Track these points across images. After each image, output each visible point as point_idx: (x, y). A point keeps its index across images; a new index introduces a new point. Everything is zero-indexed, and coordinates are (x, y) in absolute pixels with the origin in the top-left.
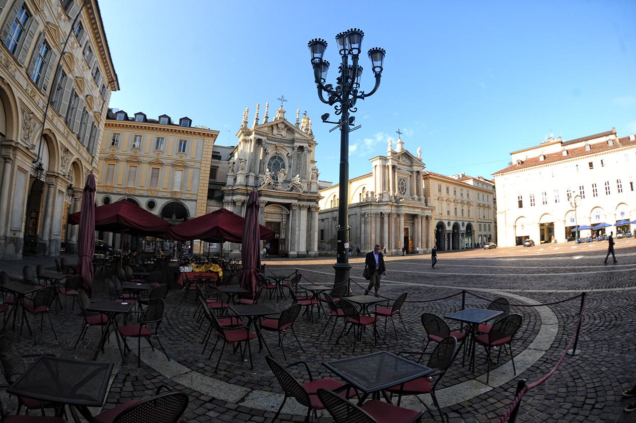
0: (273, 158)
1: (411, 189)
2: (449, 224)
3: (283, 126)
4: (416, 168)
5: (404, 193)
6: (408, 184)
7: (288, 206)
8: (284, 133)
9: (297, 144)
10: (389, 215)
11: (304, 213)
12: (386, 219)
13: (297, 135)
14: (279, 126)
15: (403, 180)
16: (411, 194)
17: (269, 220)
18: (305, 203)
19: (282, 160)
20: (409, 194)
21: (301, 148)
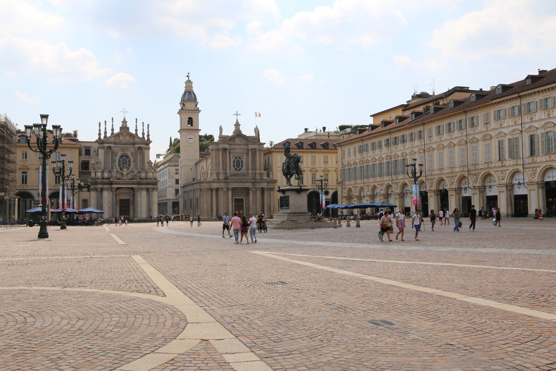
0: (122, 156)
3: (126, 134)
4: (251, 147)
6: (244, 161)
7: (132, 189)
8: (128, 138)
9: (137, 146)
10: (217, 190)
11: (144, 193)
13: (137, 140)
14: (123, 134)
15: (240, 158)
16: (248, 169)
18: (144, 186)
19: (127, 157)
20: (245, 169)
21: (140, 148)
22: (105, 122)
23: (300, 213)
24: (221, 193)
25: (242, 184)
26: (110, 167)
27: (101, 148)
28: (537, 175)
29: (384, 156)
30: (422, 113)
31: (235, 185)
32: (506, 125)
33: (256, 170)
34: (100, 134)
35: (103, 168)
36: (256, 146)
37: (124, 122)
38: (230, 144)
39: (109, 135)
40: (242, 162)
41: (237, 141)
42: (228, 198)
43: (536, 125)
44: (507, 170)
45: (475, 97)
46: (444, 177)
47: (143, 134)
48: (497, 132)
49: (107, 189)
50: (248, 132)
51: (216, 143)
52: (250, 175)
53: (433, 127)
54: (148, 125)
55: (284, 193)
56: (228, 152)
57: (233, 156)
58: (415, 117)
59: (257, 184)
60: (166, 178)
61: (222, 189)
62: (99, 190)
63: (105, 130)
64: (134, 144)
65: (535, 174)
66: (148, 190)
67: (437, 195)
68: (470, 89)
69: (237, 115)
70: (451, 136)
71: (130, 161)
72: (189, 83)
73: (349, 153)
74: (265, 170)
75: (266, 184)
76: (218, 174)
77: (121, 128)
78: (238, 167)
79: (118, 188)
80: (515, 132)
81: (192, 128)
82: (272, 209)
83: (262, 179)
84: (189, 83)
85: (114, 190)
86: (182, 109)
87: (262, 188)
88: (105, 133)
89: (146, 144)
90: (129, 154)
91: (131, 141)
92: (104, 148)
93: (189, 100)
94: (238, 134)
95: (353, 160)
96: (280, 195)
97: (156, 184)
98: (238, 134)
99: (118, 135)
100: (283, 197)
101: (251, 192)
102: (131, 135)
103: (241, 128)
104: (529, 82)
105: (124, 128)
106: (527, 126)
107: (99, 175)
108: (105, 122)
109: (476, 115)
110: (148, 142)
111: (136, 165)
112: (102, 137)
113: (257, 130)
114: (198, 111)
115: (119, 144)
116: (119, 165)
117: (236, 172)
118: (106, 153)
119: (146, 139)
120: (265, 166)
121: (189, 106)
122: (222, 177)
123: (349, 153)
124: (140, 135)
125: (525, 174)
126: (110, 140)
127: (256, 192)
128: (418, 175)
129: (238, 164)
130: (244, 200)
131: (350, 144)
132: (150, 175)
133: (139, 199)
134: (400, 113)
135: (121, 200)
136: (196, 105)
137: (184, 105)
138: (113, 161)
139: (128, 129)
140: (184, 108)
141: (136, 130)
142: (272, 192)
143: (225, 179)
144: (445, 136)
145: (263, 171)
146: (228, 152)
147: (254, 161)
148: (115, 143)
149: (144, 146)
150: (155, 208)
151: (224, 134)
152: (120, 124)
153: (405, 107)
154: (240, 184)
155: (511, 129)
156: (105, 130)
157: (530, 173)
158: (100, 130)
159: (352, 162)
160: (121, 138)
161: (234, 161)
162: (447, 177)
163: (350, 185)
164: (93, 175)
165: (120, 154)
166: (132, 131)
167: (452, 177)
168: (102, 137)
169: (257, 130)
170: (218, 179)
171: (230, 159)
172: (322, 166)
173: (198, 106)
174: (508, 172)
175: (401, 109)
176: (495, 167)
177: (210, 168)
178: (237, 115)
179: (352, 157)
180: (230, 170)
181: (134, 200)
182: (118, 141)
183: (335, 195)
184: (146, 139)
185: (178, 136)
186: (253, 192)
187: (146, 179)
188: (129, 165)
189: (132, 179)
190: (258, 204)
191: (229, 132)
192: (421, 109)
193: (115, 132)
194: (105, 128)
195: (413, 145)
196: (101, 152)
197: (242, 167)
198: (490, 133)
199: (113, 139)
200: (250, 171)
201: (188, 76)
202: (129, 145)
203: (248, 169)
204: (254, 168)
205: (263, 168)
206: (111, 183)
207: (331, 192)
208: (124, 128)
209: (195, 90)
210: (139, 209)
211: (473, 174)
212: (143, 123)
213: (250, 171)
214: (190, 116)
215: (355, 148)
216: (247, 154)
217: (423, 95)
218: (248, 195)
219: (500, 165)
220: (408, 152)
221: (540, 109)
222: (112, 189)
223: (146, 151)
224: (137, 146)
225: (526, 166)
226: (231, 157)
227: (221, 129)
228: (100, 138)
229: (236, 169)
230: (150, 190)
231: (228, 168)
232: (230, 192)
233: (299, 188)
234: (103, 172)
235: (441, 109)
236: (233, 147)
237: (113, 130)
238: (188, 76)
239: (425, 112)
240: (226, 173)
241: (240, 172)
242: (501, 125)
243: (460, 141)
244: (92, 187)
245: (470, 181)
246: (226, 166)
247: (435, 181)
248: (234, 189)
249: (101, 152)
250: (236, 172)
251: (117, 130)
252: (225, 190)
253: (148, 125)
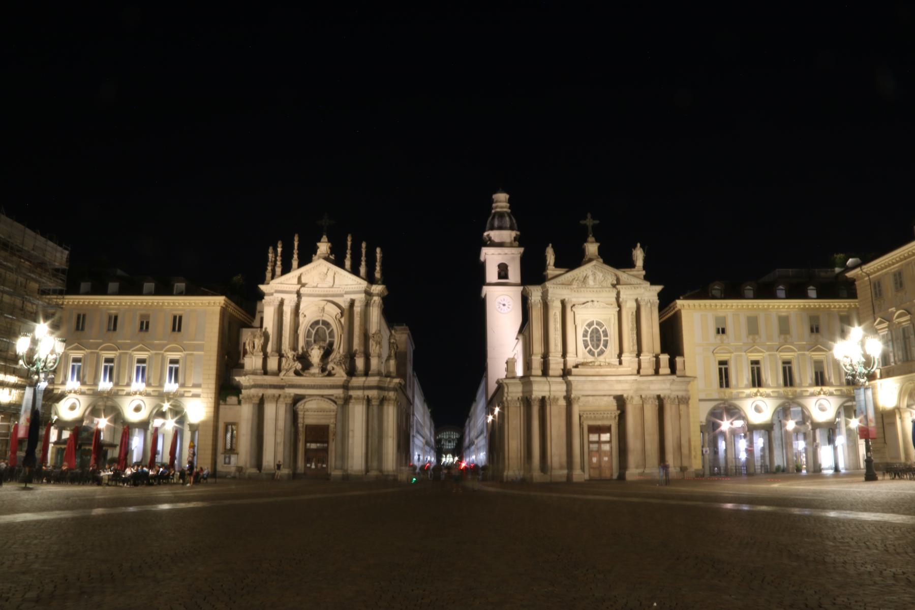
5: (601, 353)
15: (599, 324)
18: (359, 393)
40: (606, 335)
49: (277, 399)
79: (297, 399)
82: (685, 451)
117: (590, 359)
142: (682, 407)
161: (585, 335)
197: (605, 346)
226: (578, 322)
229: (590, 352)
230: (375, 403)
250: (590, 359)
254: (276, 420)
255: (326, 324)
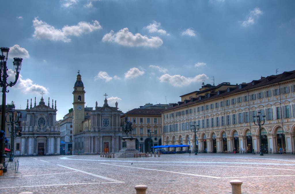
0: (40, 119)
1: (111, 123)
2: (142, 139)
3: (43, 106)
5: (107, 126)
6: (110, 121)
7: (46, 137)
8: (44, 108)
9: (49, 113)
11: (53, 139)
12: (92, 139)
13: (49, 109)
14: (41, 106)
15: (107, 119)
16: (111, 125)
17: (39, 142)
18: (52, 135)
20: (110, 126)
22: (31, 99)
23: (132, 150)
24: (96, 139)
25: (108, 134)
26: (34, 125)
27: (28, 114)
28: (256, 132)
29: (185, 119)
30: (204, 97)
31: (104, 135)
32: (242, 105)
33: (116, 126)
34: (28, 106)
35: (29, 125)
36: (116, 113)
37: (42, 99)
38: (102, 112)
39: (33, 106)
40: (108, 122)
41: (106, 110)
42: (100, 142)
43: (255, 106)
44: (244, 129)
45: (229, 90)
46: (214, 132)
47: (53, 106)
48: (238, 109)
49: (31, 137)
50: (111, 104)
51: (94, 111)
52: (113, 129)
53: (209, 104)
54: (56, 101)
55: (124, 140)
56: (100, 116)
57: (103, 118)
58: (201, 99)
59: (116, 134)
60: (65, 130)
61: (97, 136)
62: (26, 138)
63: (31, 104)
64: (47, 111)
65: (255, 131)
66: (55, 137)
67: (211, 141)
68: (231, 84)
69: (106, 95)
70: (217, 110)
71: (45, 121)
72: (79, 77)
73: (167, 117)
74: (121, 126)
75: (122, 134)
76: (94, 128)
77: (40, 103)
78: (106, 123)
79: (38, 137)
80: (246, 109)
81: (81, 102)
83: (119, 131)
84: (79, 77)
85: (35, 138)
86: (75, 91)
87: (120, 136)
88: (31, 105)
89: (54, 112)
90: (44, 117)
91: (46, 110)
92: (30, 114)
93: (78, 86)
94: (106, 105)
95: (169, 121)
96: (123, 141)
97: (60, 134)
98: (106, 105)
99: (38, 106)
100: (124, 142)
101: (113, 139)
102: (46, 106)
103: (108, 103)
104: (253, 84)
105: (42, 103)
106: (252, 106)
107: (27, 129)
108: (31, 99)
109: (229, 100)
110: (55, 110)
111: (48, 123)
112: (29, 108)
113: (117, 104)
114: (84, 92)
115: (39, 112)
116: (39, 123)
117: (105, 127)
118: (31, 117)
119: (54, 109)
120: (121, 124)
121: (79, 89)
122: (97, 130)
123: (167, 117)
124: (51, 107)
125: (251, 131)
126: (34, 110)
127: (116, 138)
128: (197, 130)
129: (106, 123)
130: (109, 143)
131: (168, 112)
132: (56, 130)
133: (49, 143)
134: (194, 96)
135: (38, 143)
136: (83, 89)
137: (76, 88)
138: (35, 121)
139: (44, 103)
140: (76, 91)
141: (49, 104)
143: (99, 131)
144: (215, 110)
145: (120, 127)
146: (100, 116)
147: (115, 121)
148: (36, 111)
149: (53, 113)
150: (59, 147)
151: (98, 106)
152: (40, 101)
153: (197, 93)
154: (107, 134)
155: (245, 107)
156: (31, 104)
157: (253, 130)
158: (28, 104)
159: (169, 122)
160: (40, 108)
161: (104, 121)
162: (215, 132)
163: (168, 135)
164: (23, 130)
165: (39, 117)
166: (46, 104)
167: (218, 131)
168: (29, 108)
169: (117, 104)
170: (95, 131)
171: (102, 120)
172: (154, 124)
173: (84, 89)
174: (243, 130)
175: (195, 94)
176: (238, 127)
177: (90, 125)
178: (106, 95)
179: (169, 120)
180: (101, 126)
181: (46, 143)
182: (38, 110)
183: (160, 140)
184: (54, 109)
185: (72, 107)
186: (114, 138)
187: (54, 131)
188: (44, 124)
189: (46, 131)
190: (117, 145)
191: (101, 105)
192: (203, 95)
193: (37, 105)
194: (31, 103)
195: (199, 114)
196: (29, 117)
197: (108, 124)
198: (235, 109)
199: (35, 109)
200: (113, 127)
201: (78, 72)
202: (44, 112)
203: (111, 125)
204: (115, 125)
205: (120, 125)
206: (34, 134)
207: (158, 139)
208: (42, 103)
209: (83, 80)
210: (49, 148)
211: (227, 130)
212: (53, 100)
213: (113, 127)
214: (80, 95)
215: (170, 114)
216: (111, 117)
217: (208, 86)
218: (111, 140)
219: (240, 126)
220: (197, 117)
221: (265, 96)
222: (34, 137)
223: (54, 116)
224: (49, 113)
225: (252, 127)
226: (102, 119)
227: (97, 103)
228: (27, 108)
231: (100, 125)
232: (101, 139)
233: (131, 137)
234: (29, 128)
235: (214, 95)
236: (103, 113)
237: (35, 104)
238: (78, 72)
239: (206, 96)
240: (99, 128)
241: (107, 127)
242: (240, 105)
243: (221, 113)
244: (23, 136)
245: (227, 134)
246: (99, 124)
247: (210, 133)
248: (103, 137)
249: (29, 117)
250: (105, 127)
251: (38, 104)
252: (99, 137)
253: (56, 101)
254: (32, 142)
255: (43, 119)
